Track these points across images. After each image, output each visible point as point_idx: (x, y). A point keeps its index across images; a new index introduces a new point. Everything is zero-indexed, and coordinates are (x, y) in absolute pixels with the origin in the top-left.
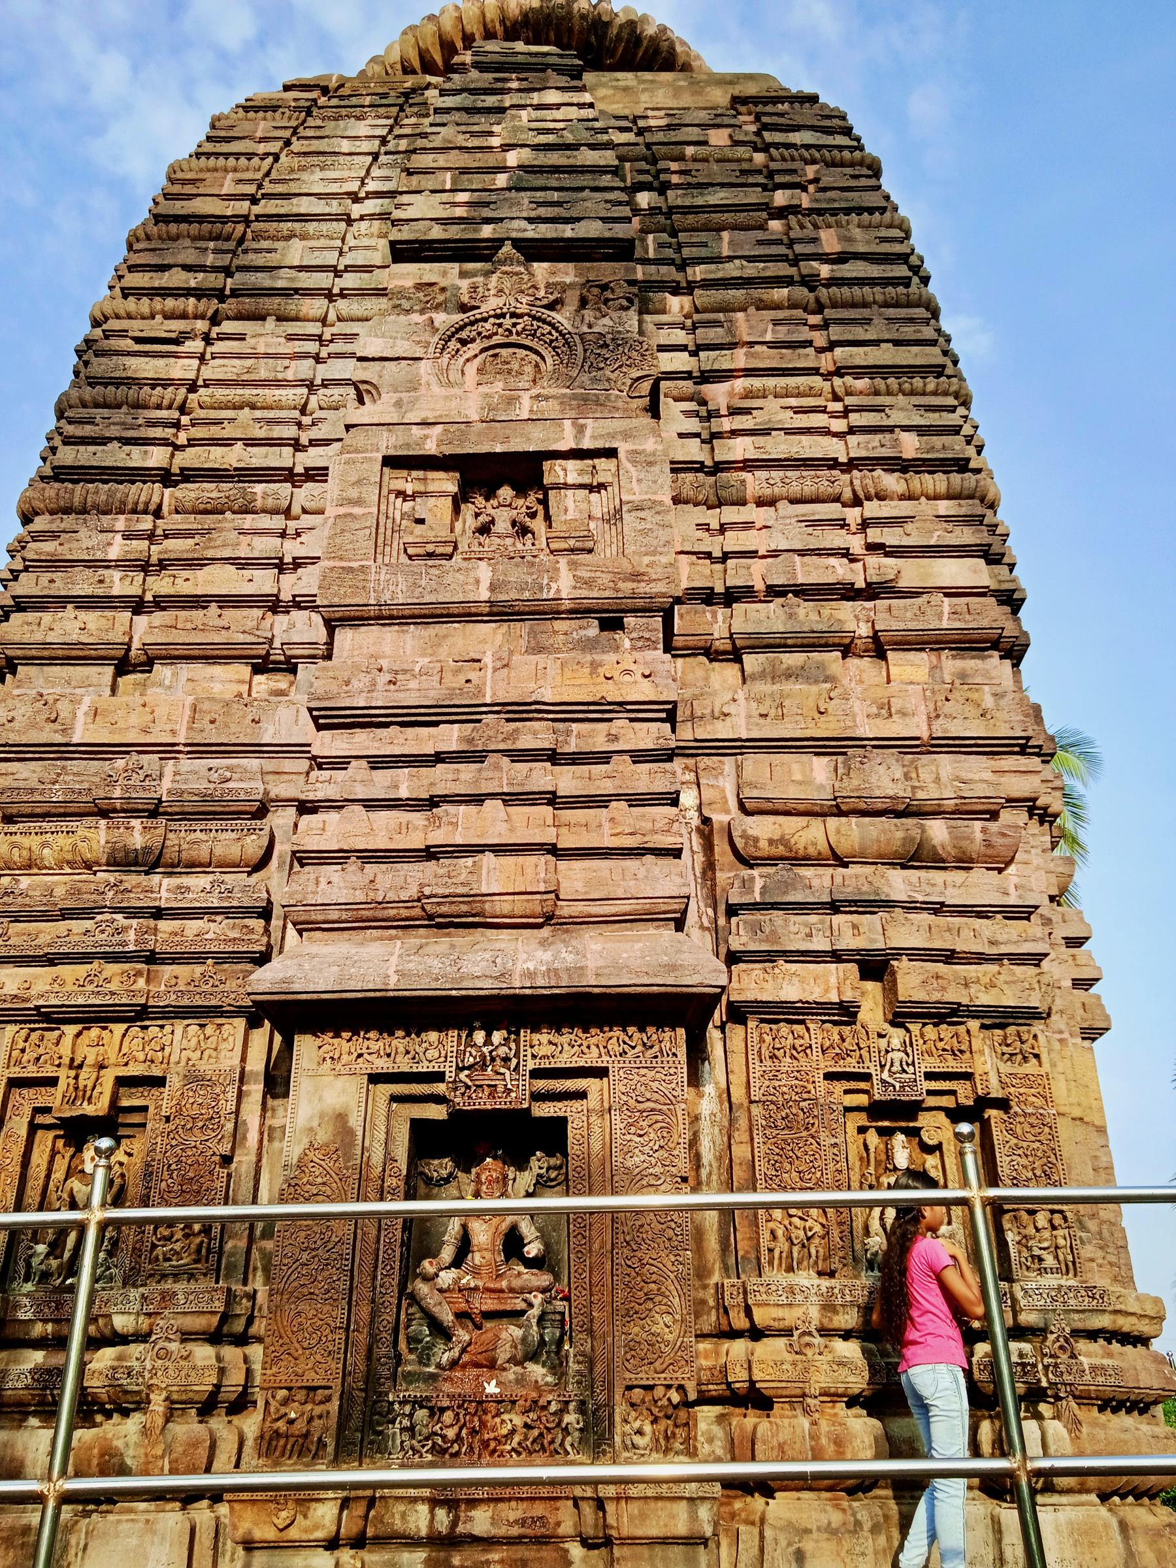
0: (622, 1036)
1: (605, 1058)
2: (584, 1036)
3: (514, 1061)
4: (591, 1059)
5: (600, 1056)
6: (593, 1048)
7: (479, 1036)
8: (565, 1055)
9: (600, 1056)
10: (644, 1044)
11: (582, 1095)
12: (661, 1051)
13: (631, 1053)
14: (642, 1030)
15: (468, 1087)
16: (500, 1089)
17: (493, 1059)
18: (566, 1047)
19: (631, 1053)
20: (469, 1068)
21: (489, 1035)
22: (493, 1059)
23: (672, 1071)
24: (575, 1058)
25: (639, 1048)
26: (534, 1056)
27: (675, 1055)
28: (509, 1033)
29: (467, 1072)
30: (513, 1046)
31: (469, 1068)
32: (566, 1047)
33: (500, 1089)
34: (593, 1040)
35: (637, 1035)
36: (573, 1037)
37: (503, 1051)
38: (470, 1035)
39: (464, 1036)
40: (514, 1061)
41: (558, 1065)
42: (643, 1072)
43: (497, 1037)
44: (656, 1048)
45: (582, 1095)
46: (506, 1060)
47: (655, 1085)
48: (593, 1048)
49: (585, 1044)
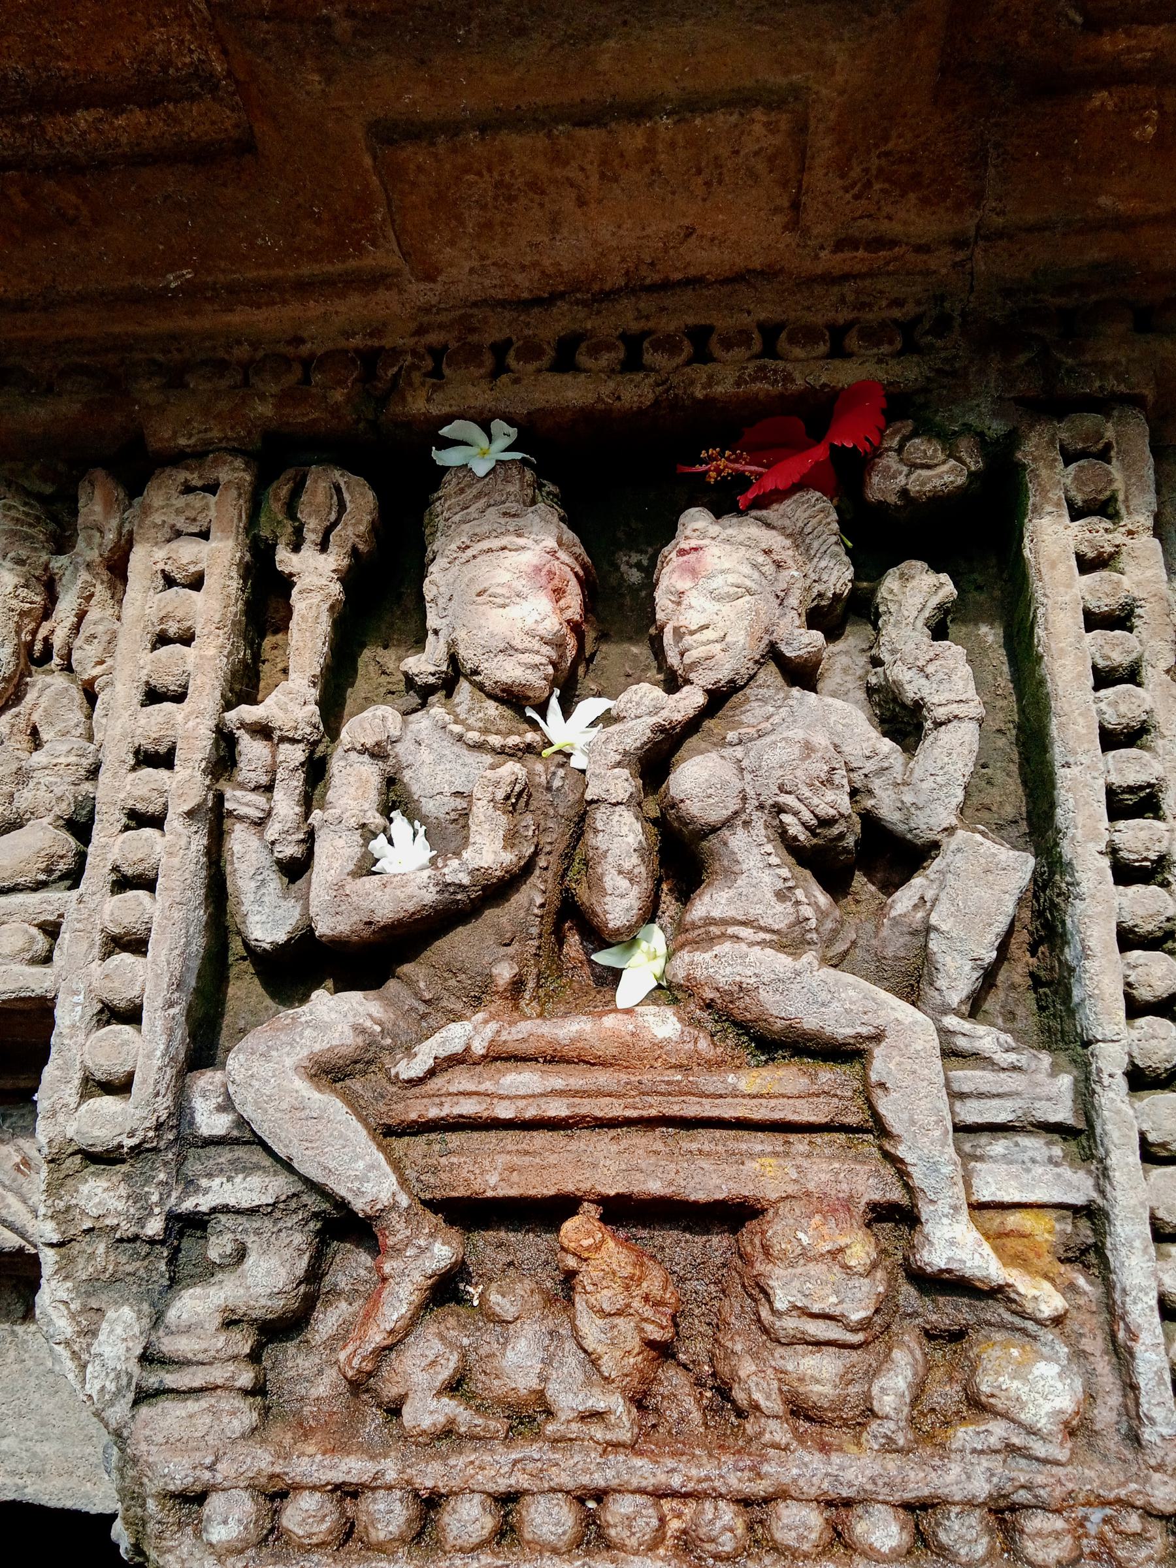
3: (972, 892)
7: (504, 586)
15: (343, 1226)
16: (820, 1271)
17: (682, 858)
20: (367, 959)
21: (615, 611)
22: (682, 858)
28: (879, 538)
29: (336, 1016)
30: (952, 681)
31: (367, 959)
33: (820, 1271)
37: (812, 743)
38: (384, 597)
39: (315, 577)
40: (972, 892)
43: (724, 581)
46: (863, 856)
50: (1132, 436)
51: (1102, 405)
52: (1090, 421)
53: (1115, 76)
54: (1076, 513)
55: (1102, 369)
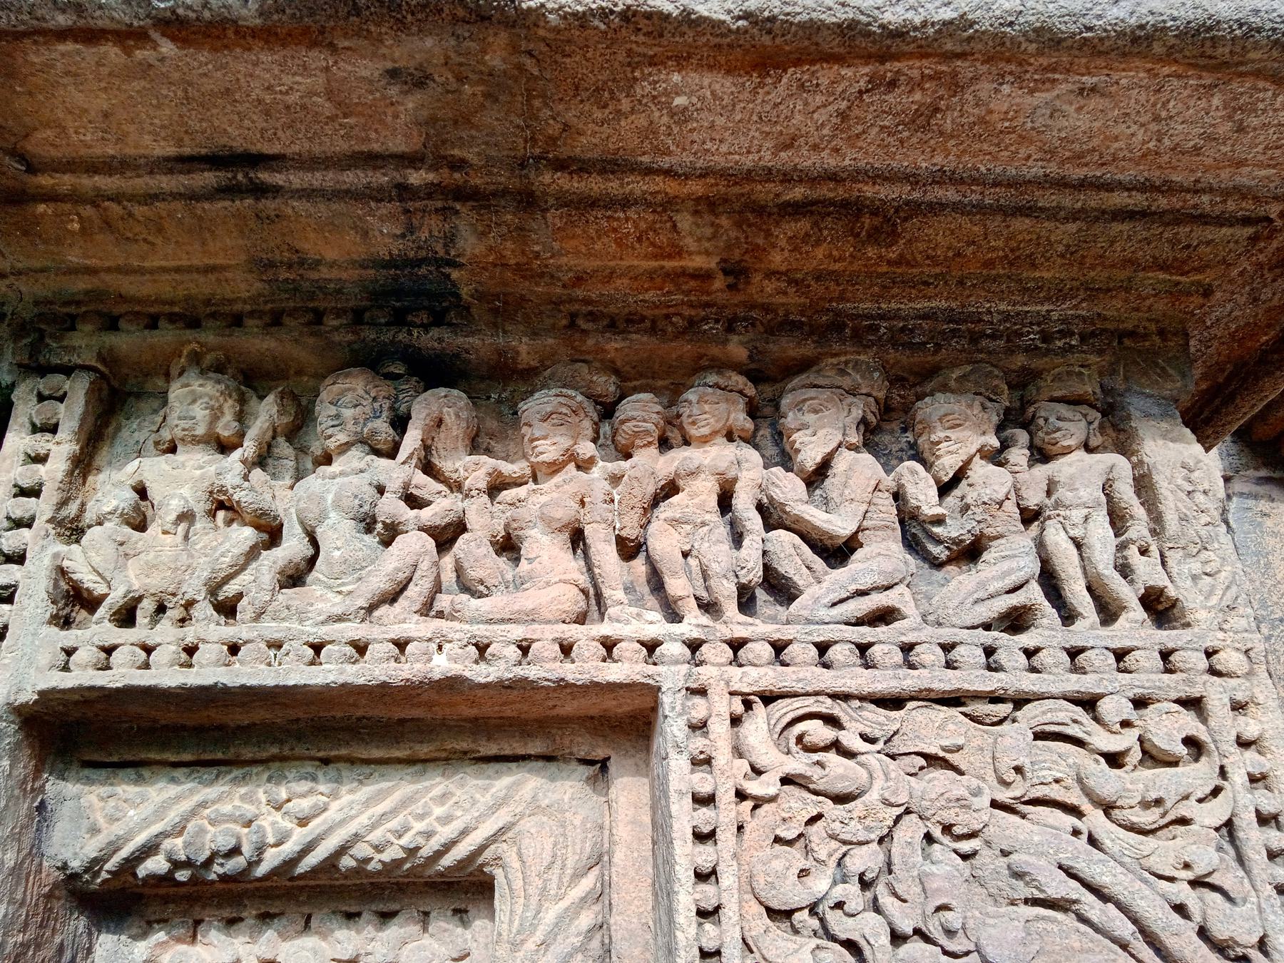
0: (752, 472)
1: (634, 621)
2: (475, 469)
4: (523, 617)
5: (595, 601)
6: (545, 550)
8: (320, 596)
9: (595, 601)
10: (914, 531)
11: (462, 888)
12: (1049, 580)
13: (821, 588)
14: (889, 429)
18: (340, 538)
19: (821, 588)
23: (1167, 728)
24: (402, 619)
25: (883, 556)
26: (74, 601)
27: (1160, 608)
32: (340, 538)
34: (551, 498)
35: (859, 471)
36: (396, 472)
41: (251, 672)
42: (931, 728)
44: (1011, 559)
45: (462, 888)
47: (1041, 841)
48: (545, 550)
49: (484, 520)
50: (78, 389)
51: (67, 371)
52: (57, 379)
53: (51, 197)
54: (35, 429)
55: (71, 350)
